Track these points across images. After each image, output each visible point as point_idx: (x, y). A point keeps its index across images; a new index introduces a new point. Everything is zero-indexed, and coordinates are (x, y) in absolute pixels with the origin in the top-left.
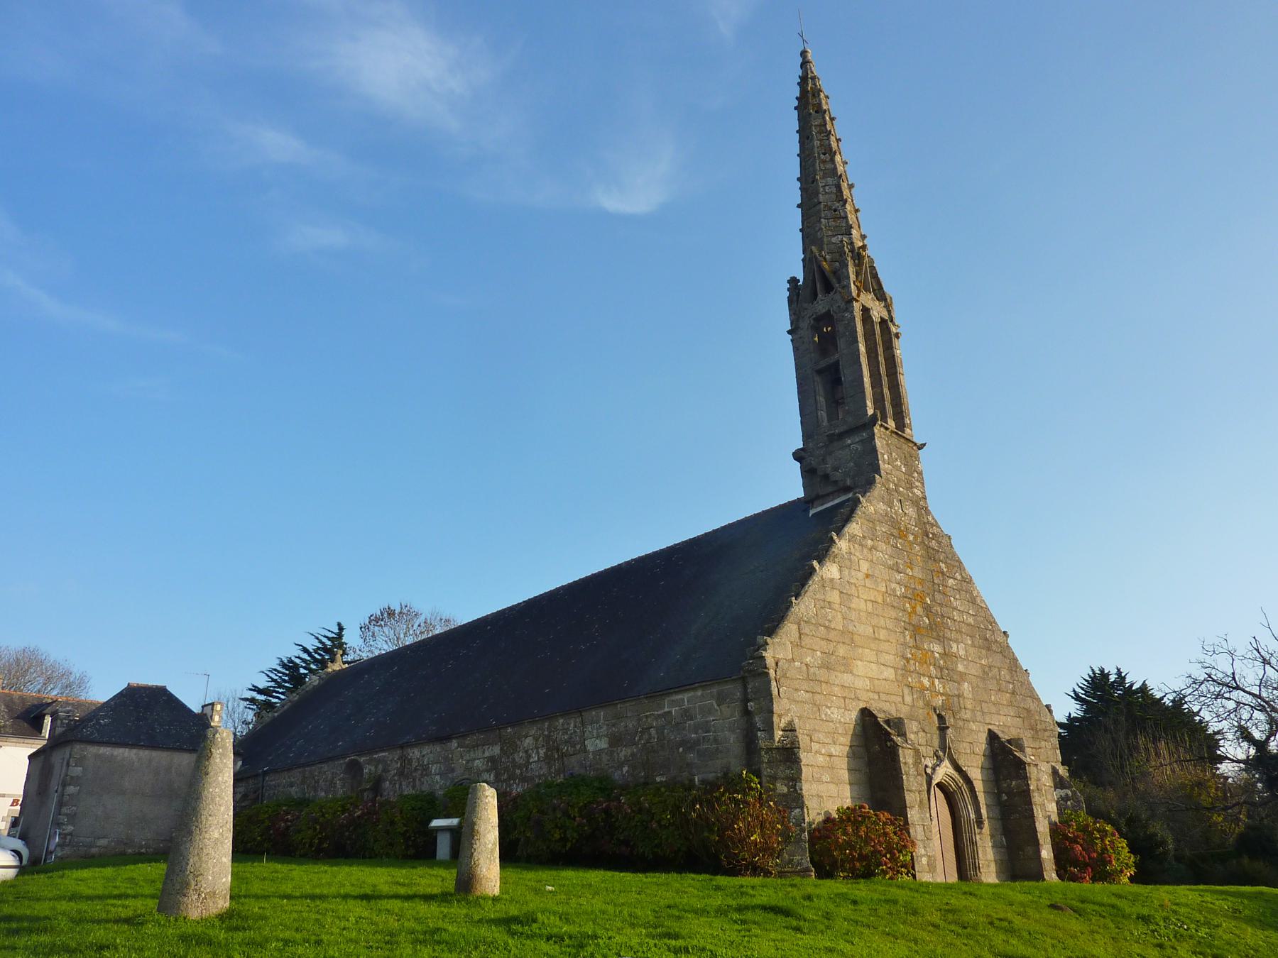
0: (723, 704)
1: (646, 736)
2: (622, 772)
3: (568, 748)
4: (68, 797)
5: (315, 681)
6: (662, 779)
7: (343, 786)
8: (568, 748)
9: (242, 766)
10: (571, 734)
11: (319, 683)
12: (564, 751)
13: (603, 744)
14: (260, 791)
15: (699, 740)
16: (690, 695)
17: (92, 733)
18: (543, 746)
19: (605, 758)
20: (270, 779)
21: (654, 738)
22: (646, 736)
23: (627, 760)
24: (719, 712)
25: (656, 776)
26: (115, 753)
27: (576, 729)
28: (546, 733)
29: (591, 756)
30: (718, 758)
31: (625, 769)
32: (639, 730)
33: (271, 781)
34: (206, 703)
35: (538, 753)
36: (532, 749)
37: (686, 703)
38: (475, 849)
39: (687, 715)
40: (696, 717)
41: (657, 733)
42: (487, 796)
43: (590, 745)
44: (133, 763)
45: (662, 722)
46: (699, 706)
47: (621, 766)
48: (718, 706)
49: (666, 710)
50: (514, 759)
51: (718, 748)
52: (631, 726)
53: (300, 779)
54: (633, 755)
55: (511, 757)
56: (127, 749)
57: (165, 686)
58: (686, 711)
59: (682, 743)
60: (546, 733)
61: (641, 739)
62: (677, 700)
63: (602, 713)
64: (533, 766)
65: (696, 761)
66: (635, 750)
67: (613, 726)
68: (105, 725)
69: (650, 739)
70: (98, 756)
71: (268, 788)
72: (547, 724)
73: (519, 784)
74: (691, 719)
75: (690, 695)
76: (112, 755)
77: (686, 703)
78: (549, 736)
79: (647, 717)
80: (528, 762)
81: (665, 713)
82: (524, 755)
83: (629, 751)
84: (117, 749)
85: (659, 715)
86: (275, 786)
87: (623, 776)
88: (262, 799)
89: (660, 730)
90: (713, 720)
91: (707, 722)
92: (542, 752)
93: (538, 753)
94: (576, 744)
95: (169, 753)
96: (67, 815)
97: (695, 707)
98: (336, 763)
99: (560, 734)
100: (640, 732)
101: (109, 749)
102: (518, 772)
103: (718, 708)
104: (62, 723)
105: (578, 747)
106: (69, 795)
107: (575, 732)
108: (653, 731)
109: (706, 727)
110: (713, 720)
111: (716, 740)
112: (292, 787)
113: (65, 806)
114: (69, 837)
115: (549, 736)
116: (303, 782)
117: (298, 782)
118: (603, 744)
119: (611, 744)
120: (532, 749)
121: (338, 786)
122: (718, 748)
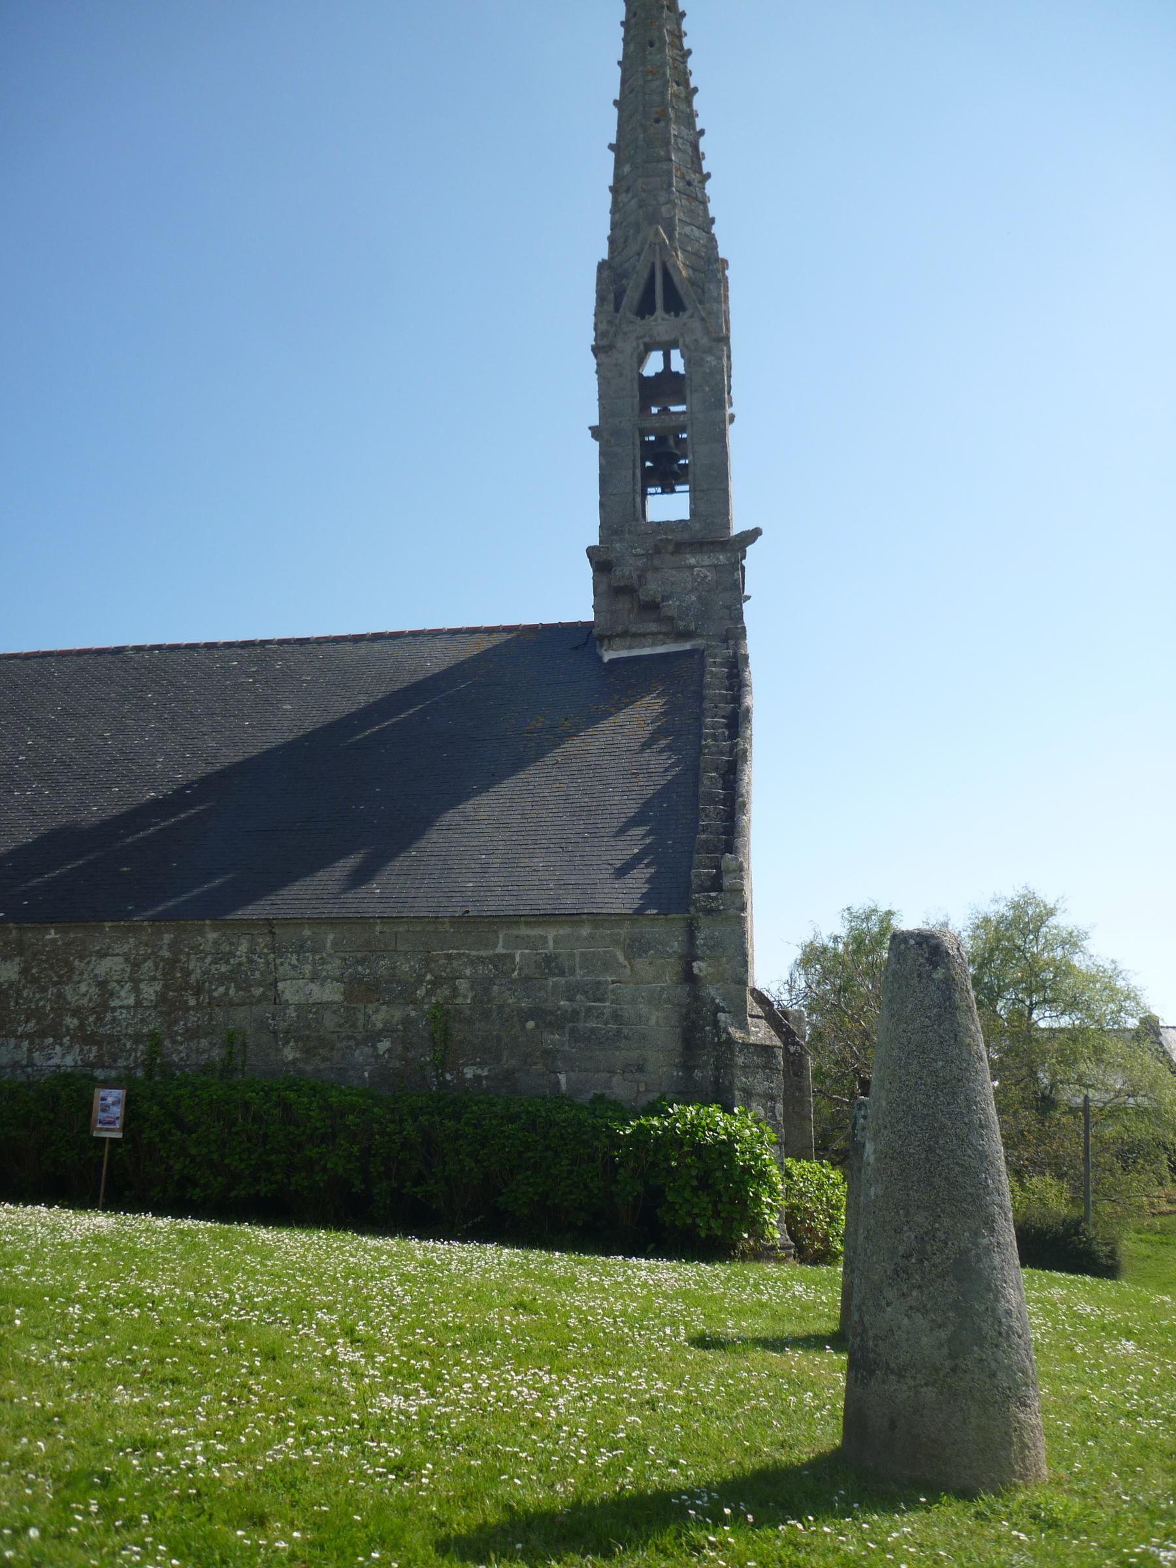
0: (640, 956)
1: (444, 991)
2: (375, 1048)
3: (227, 989)
6: (479, 1072)
8: (227, 989)
10: (240, 964)
12: (216, 994)
13: (331, 993)
15: (575, 1013)
16: (561, 932)
18: (154, 978)
19: (330, 1020)
21: (465, 997)
22: (444, 991)
23: (388, 1031)
24: (628, 971)
25: (465, 1065)
27: (255, 957)
28: (166, 954)
29: (292, 1012)
30: (618, 1048)
31: (384, 1045)
32: (429, 977)
35: (136, 990)
36: (118, 982)
37: (551, 943)
39: (550, 964)
40: (573, 971)
41: (472, 988)
43: (290, 991)
45: (487, 970)
46: (582, 953)
47: (374, 1037)
48: (626, 958)
49: (500, 950)
50: (60, 996)
51: (619, 1031)
52: (406, 968)
54: (407, 1021)
55: (52, 991)
58: (548, 959)
59: (533, 1014)
60: (166, 954)
61: (429, 993)
62: (528, 936)
63: (331, 937)
64: (120, 1015)
65: (567, 1048)
66: (413, 1014)
67: (361, 962)
69: (455, 997)
72: (167, 938)
73: (70, 1047)
74: (562, 973)
75: (561, 932)
77: (551, 943)
78: (172, 963)
79: (449, 957)
80: (102, 1008)
81: (497, 955)
82: (94, 990)
83: (398, 1014)
85: (479, 958)
87: (378, 1056)
89: (482, 986)
90: (613, 982)
91: (599, 983)
92: (150, 991)
93: (136, 990)
94: (251, 986)
97: (572, 955)
99: (209, 959)
100: (429, 982)
102: (72, 1022)
103: (626, 963)
105: (258, 991)
107: (251, 961)
108: (463, 985)
109: (597, 992)
110: (613, 982)
111: (616, 1016)
115: (172, 963)
118: (331, 993)
119: (348, 996)
120: (118, 982)
122: (619, 1031)
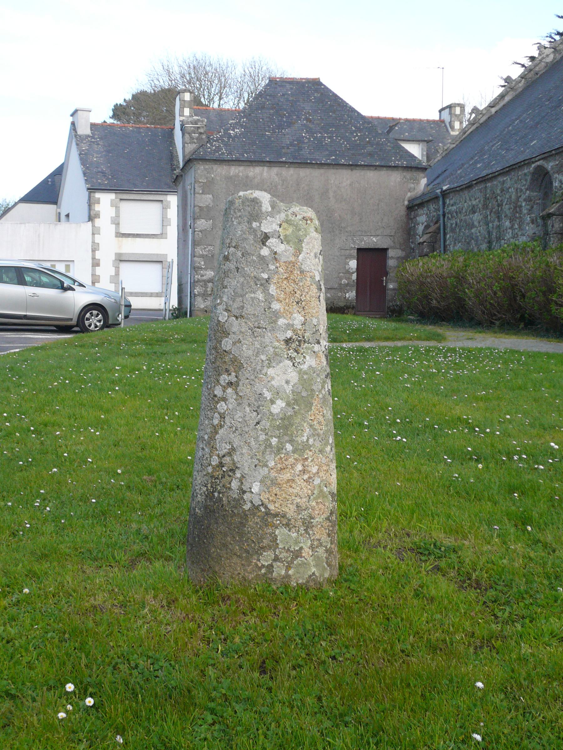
4: (200, 233)
5: (547, 56)
7: (530, 211)
9: (428, 185)
11: (554, 58)
14: (441, 221)
17: (218, 149)
20: (452, 202)
26: (251, 174)
33: (452, 205)
34: (444, 106)
38: (222, 417)
42: (266, 237)
44: (276, 186)
53: (482, 202)
56: (266, 168)
57: (319, 78)
68: (236, 136)
70: (229, 179)
71: (450, 216)
76: (247, 177)
84: (252, 169)
86: (456, 212)
88: (444, 232)
95: (322, 171)
96: (202, 256)
98: (520, 173)
101: (241, 168)
104: (192, 138)
106: (201, 231)
112: (474, 212)
113: (198, 245)
114: (210, 285)
116: (485, 206)
117: (480, 206)
121: (525, 211)
